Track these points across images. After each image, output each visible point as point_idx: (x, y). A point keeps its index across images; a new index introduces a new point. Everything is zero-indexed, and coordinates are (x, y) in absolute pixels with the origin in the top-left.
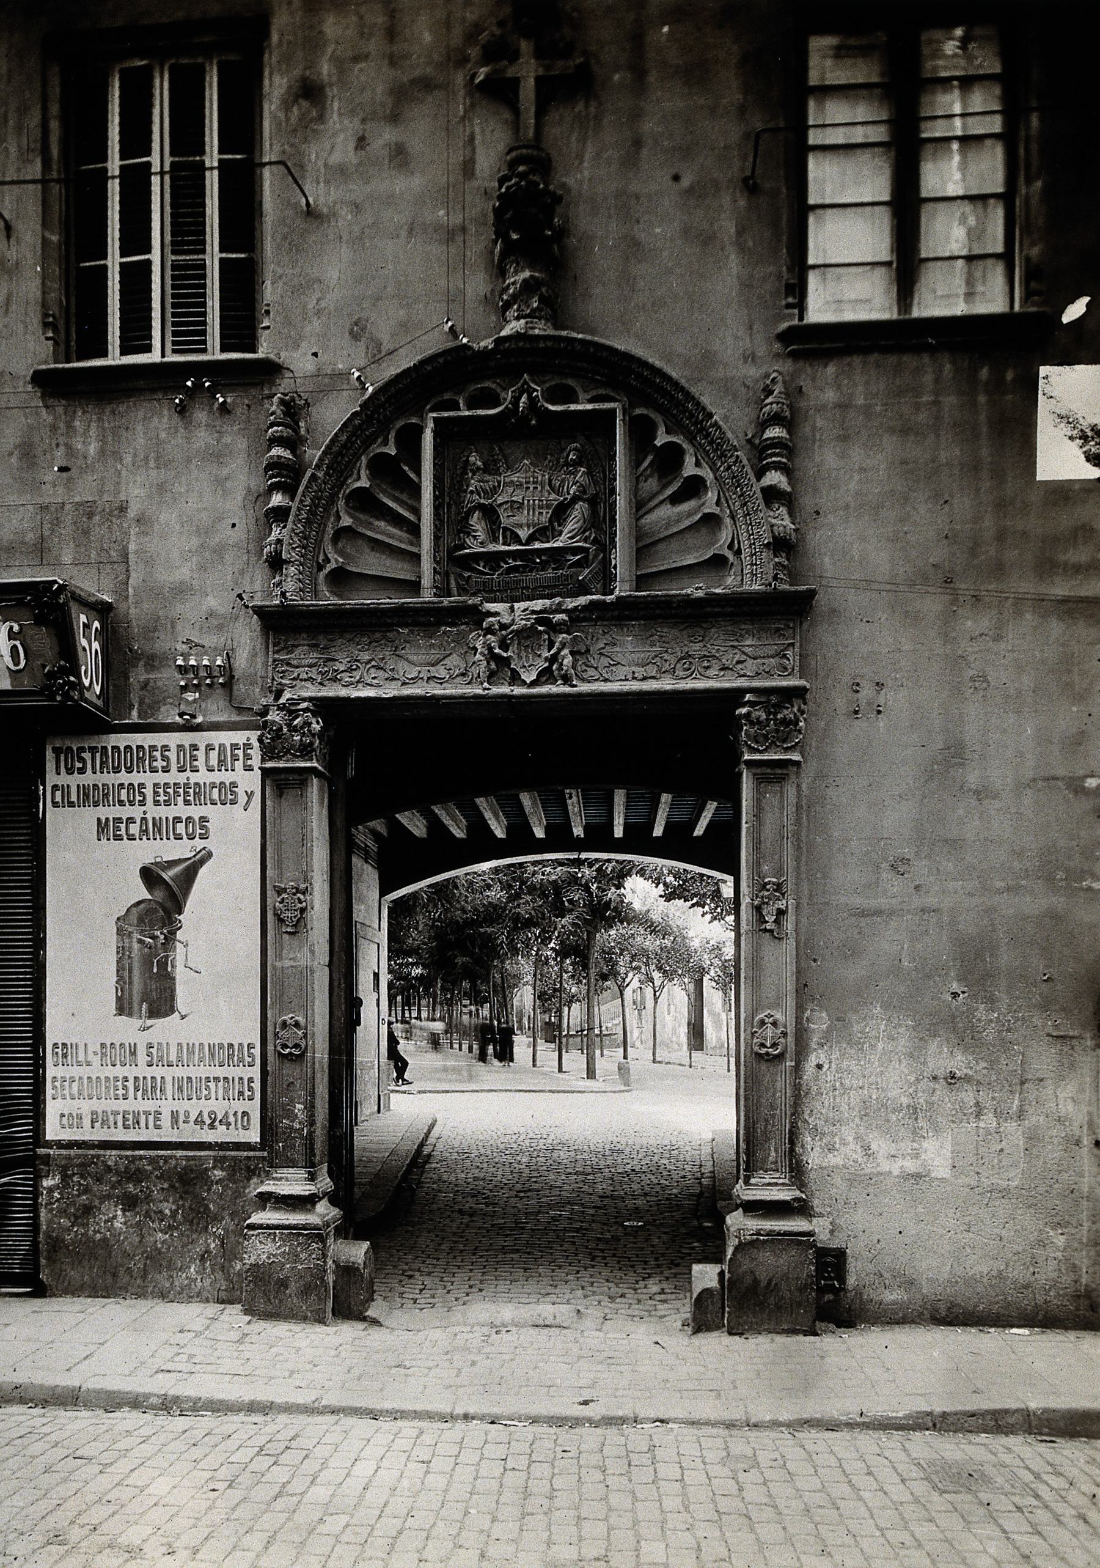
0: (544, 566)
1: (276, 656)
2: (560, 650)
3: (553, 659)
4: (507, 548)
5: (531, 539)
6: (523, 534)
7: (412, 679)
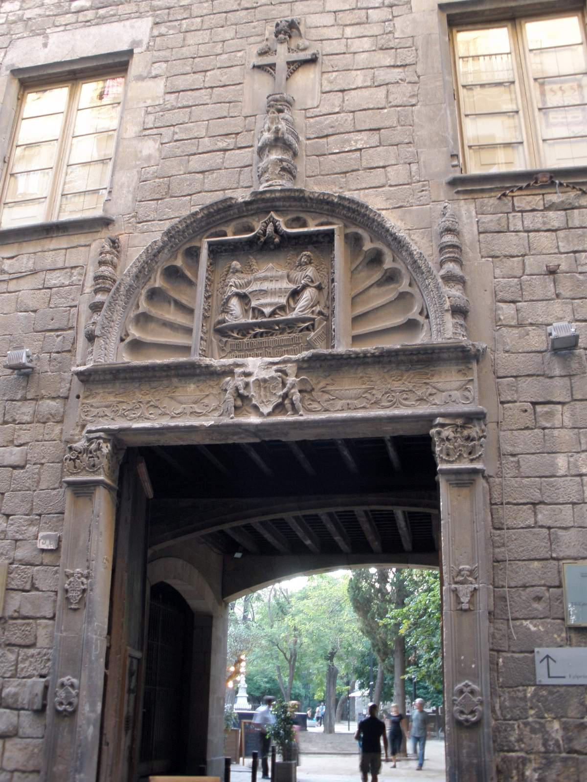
0: (282, 331)
2: (290, 389)
3: (285, 396)
4: (254, 320)
5: (273, 314)
6: (267, 310)
7: (178, 414)
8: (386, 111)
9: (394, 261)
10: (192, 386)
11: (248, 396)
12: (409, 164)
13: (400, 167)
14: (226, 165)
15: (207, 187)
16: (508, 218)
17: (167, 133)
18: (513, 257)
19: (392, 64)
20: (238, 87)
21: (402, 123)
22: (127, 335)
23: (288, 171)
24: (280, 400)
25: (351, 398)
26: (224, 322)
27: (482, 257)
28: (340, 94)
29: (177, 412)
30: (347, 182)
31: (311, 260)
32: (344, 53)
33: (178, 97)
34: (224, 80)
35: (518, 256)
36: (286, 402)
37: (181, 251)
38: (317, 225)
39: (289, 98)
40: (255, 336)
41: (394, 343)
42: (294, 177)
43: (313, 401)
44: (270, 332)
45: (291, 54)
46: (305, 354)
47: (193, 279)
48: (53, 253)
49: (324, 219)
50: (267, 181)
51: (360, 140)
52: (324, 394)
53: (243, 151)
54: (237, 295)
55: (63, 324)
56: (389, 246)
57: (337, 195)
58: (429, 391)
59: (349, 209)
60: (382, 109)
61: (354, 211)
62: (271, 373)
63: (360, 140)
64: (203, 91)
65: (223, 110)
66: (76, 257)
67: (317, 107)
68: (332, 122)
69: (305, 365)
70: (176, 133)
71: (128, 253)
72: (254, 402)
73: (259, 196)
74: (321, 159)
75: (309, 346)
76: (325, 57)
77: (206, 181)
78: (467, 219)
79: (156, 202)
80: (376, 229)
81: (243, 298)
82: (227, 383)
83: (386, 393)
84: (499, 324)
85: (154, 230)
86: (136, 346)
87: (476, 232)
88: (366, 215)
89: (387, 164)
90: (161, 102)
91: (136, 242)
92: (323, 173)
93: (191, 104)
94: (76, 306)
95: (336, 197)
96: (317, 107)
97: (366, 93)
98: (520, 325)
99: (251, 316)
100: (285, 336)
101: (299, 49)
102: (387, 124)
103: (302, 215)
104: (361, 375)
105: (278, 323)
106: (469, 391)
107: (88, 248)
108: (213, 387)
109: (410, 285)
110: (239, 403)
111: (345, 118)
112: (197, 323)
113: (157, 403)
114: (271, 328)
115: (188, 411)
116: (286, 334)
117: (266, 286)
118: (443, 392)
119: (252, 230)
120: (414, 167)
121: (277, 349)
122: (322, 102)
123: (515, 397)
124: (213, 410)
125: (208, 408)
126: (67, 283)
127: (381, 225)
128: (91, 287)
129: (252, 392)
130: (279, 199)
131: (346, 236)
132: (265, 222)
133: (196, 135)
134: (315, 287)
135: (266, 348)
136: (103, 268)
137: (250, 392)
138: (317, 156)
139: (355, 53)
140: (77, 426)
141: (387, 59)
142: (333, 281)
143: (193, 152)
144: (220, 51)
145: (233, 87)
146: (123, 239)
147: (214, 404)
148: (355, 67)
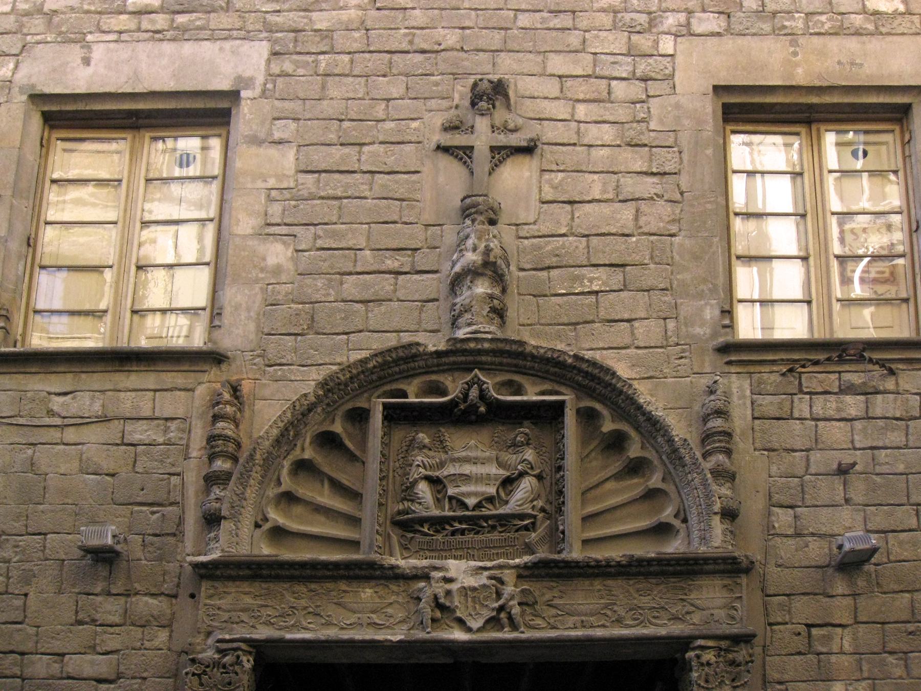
1: (208, 601)
3: (501, 608)
4: (452, 514)
5: (479, 506)
6: (471, 501)
8: (634, 239)
9: (642, 448)
10: (369, 591)
11: (449, 607)
12: (665, 319)
13: (652, 323)
14: (401, 294)
15: (372, 324)
16: (792, 402)
17: (305, 236)
18: (796, 451)
19: (644, 169)
20: (414, 177)
21: (657, 260)
22: (266, 519)
23: (499, 313)
24: (494, 613)
25: (586, 615)
26: (408, 514)
27: (755, 450)
28: (568, 207)
29: (348, 622)
30: (577, 338)
31: (529, 439)
32: (575, 144)
33: (319, 181)
34: (391, 162)
35: (803, 451)
36: (503, 615)
37: (340, 413)
38: (537, 394)
39: (496, 205)
40: (453, 533)
41: (646, 550)
42: (504, 323)
43: (536, 616)
44: (474, 529)
45: (495, 134)
46: (527, 559)
47: (358, 453)
48: (133, 394)
49: (547, 386)
50: (469, 325)
51: (598, 279)
52: (551, 609)
53: (425, 276)
54: (428, 478)
55: (161, 496)
56: (637, 428)
57: (572, 353)
58: (686, 609)
59: (587, 374)
60: (628, 235)
61: (593, 378)
62: (483, 579)
63: (598, 279)
64: (357, 176)
65: (393, 210)
66: (170, 405)
67: (535, 223)
68: (558, 248)
69: (526, 573)
70: (320, 237)
71: (256, 407)
72: (458, 614)
73: (458, 346)
74: (541, 301)
75: (529, 549)
76: (545, 147)
77: (370, 315)
78: (739, 399)
79: (293, 337)
80: (623, 405)
81: (434, 482)
82: (420, 590)
83: (631, 610)
84: (772, 532)
85: (293, 378)
86: (278, 533)
87: (749, 417)
88: (610, 384)
89: (634, 317)
90: (292, 185)
91: (267, 392)
92: (542, 321)
93: (340, 194)
94: (178, 475)
95: (569, 356)
96: (535, 223)
97: (605, 209)
98: (798, 535)
99: (447, 507)
100: (495, 536)
101: (506, 129)
102: (636, 258)
103: (517, 378)
104: (599, 587)
105: (486, 518)
106: (736, 610)
107: (191, 393)
108: (398, 594)
109: (664, 480)
110: (438, 614)
111: (575, 244)
112: (368, 511)
113: (318, 610)
114: (476, 524)
115: (365, 620)
116: (496, 533)
117: (467, 469)
118: (703, 610)
119: (444, 393)
120: (671, 324)
121: (485, 551)
122: (542, 216)
123: (787, 619)
124: (400, 622)
125: (392, 620)
126: (161, 440)
127: (631, 400)
128: (200, 450)
129: (457, 601)
130: (486, 352)
131: (578, 411)
132: (467, 383)
133: (351, 244)
134: (534, 476)
135: (468, 548)
136: (220, 424)
137: (451, 602)
138: (534, 296)
139: (591, 146)
140: (199, 633)
141: (636, 161)
142: (560, 468)
143: (348, 270)
144: (381, 115)
145: (406, 176)
146: (246, 387)
147: (401, 615)
148: (590, 169)
